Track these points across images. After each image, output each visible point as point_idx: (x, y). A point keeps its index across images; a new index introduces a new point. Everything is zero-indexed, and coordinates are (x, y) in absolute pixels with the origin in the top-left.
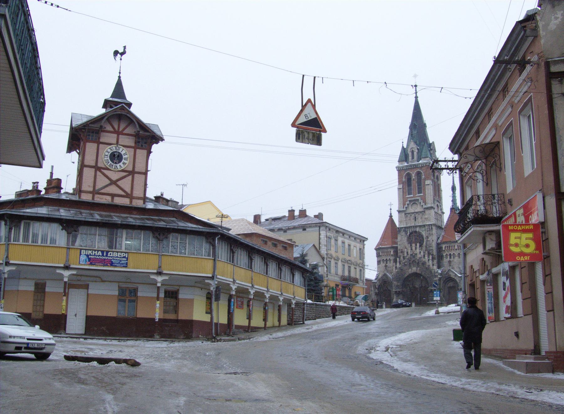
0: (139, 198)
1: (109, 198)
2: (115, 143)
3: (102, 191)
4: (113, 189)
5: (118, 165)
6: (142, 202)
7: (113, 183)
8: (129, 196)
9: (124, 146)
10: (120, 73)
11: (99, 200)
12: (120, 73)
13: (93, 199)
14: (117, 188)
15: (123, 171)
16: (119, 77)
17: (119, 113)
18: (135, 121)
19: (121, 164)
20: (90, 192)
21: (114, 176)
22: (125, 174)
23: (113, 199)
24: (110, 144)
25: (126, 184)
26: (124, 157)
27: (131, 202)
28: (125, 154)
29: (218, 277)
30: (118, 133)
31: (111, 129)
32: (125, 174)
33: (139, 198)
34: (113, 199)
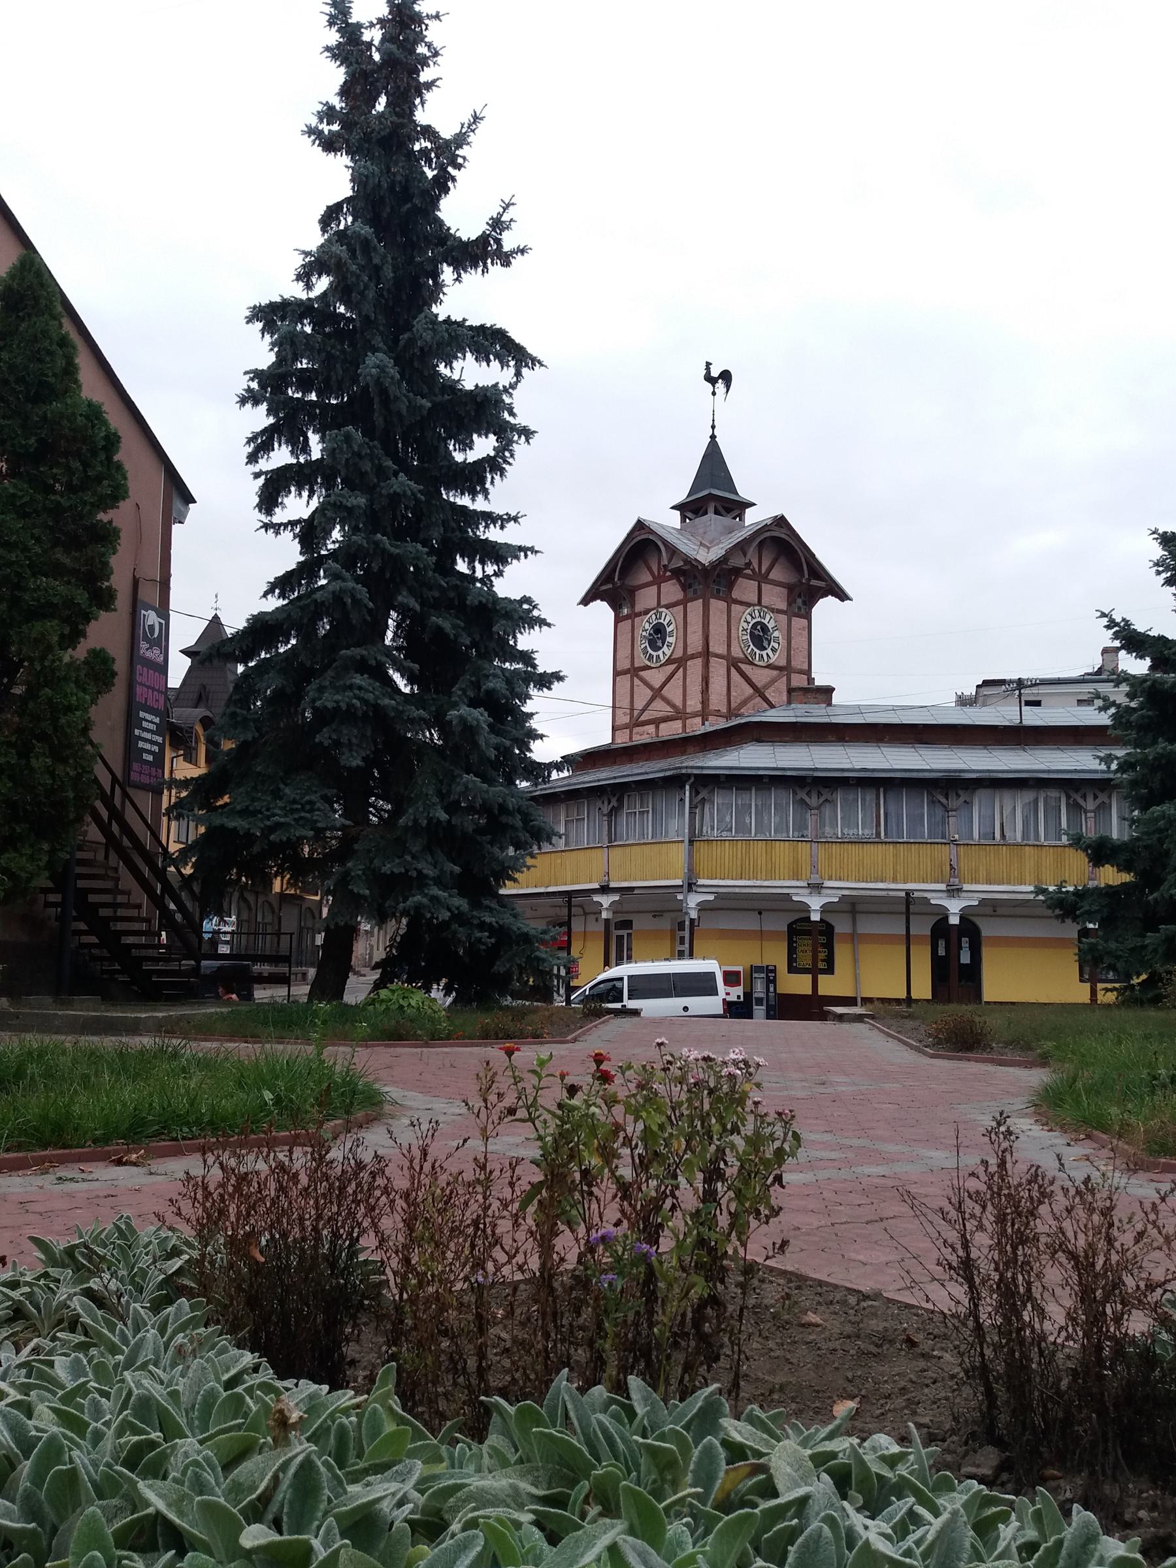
0: (695, 715)
1: (651, 729)
2: (654, 603)
3: (642, 718)
4: (660, 708)
5: (660, 653)
6: (699, 720)
7: (657, 693)
8: (680, 714)
9: (667, 607)
10: (713, 427)
11: (638, 737)
12: (713, 427)
13: (631, 738)
14: (662, 703)
15: (669, 661)
16: (713, 437)
17: (639, 538)
18: (660, 543)
19: (665, 648)
20: (625, 726)
21: (656, 677)
22: (673, 667)
23: (657, 728)
24: (646, 612)
25: (673, 691)
26: (669, 630)
27: (684, 726)
28: (669, 624)
29: (701, 882)
30: (658, 581)
31: (650, 578)
32: (673, 667)
33: (695, 715)
34: (657, 728)
